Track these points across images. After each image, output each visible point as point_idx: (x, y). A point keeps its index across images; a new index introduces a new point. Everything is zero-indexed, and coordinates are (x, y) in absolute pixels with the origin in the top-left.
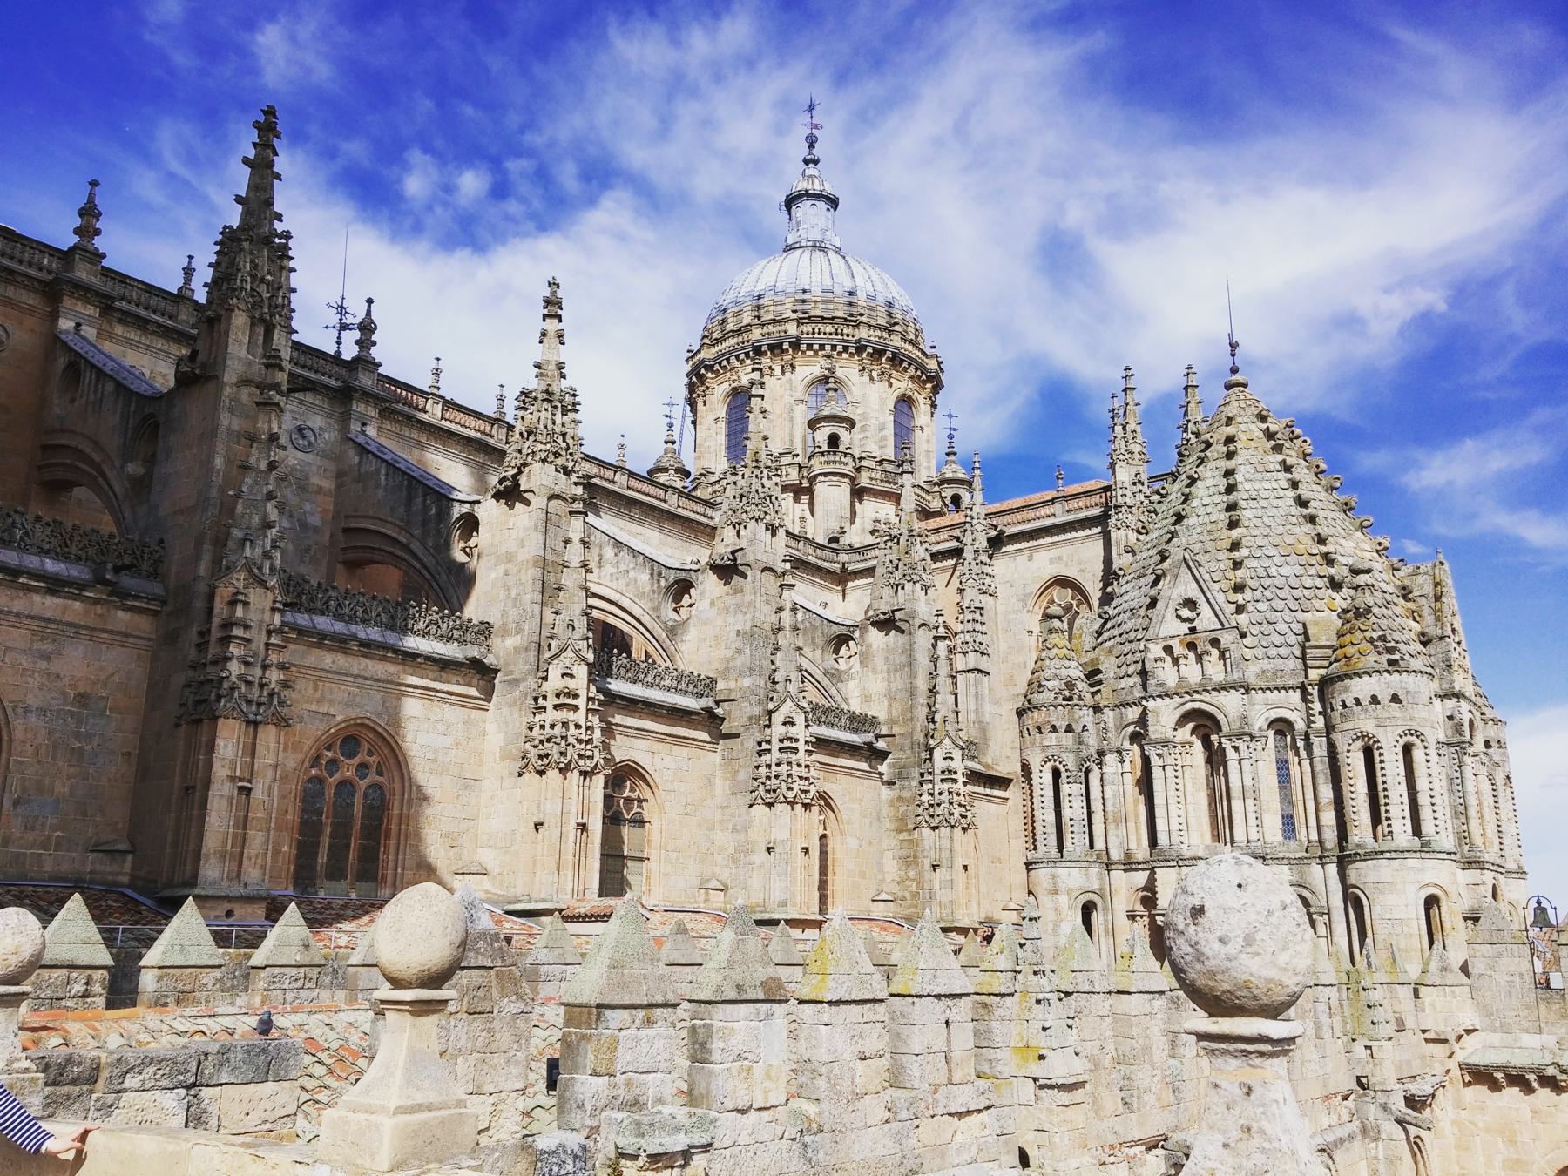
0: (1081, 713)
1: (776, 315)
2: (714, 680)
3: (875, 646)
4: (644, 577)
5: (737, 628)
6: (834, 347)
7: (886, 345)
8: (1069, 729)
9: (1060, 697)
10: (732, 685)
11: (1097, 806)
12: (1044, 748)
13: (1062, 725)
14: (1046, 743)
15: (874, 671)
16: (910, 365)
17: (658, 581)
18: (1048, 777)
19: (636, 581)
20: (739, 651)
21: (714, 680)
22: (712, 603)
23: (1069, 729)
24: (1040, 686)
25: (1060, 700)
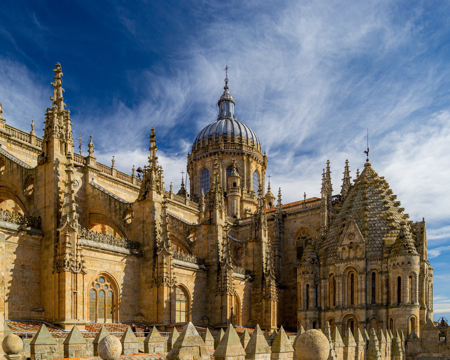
0: (316, 268)
1: (216, 142)
2: (204, 260)
3: (250, 249)
4: (181, 228)
5: (211, 243)
6: (234, 153)
7: (250, 152)
8: (312, 273)
9: (310, 263)
10: (210, 261)
11: (319, 295)
12: (305, 279)
13: (310, 271)
14: (306, 277)
15: (249, 257)
16: (258, 159)
17: (186, 229)
18: (305, 287)
19: (179, 229)
20: (211, 251)
21: (204, 260)
22: (203, 236)
23: (312, 273)
24: (305, 260)
25: (310, 264)
